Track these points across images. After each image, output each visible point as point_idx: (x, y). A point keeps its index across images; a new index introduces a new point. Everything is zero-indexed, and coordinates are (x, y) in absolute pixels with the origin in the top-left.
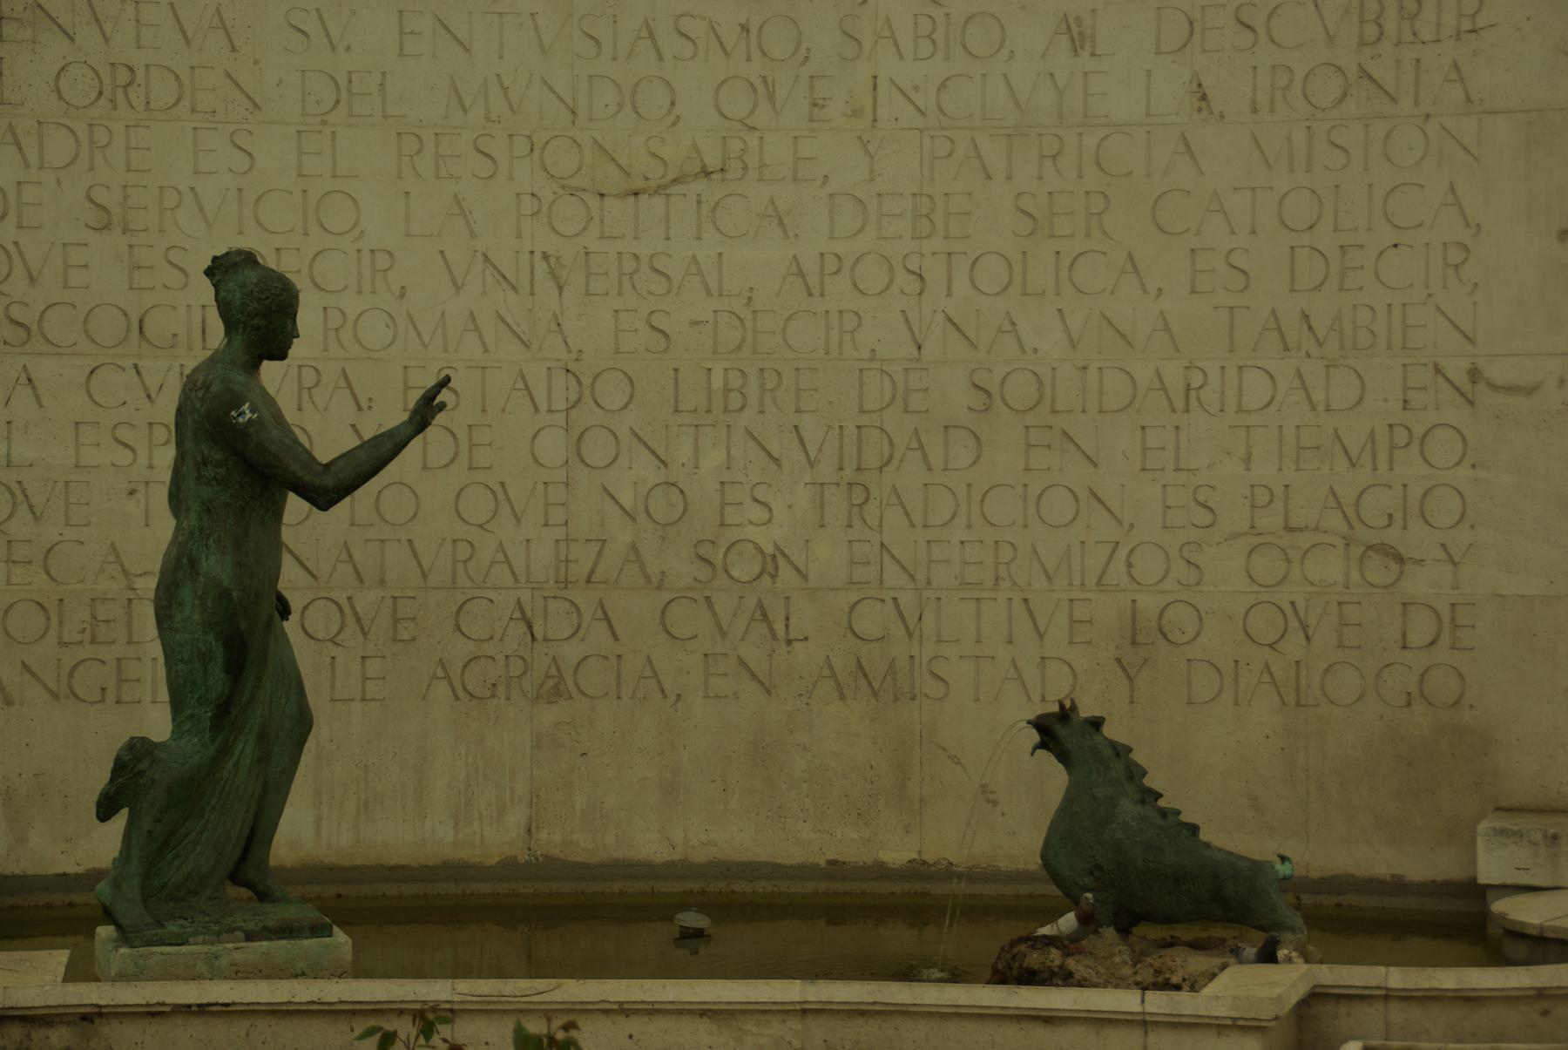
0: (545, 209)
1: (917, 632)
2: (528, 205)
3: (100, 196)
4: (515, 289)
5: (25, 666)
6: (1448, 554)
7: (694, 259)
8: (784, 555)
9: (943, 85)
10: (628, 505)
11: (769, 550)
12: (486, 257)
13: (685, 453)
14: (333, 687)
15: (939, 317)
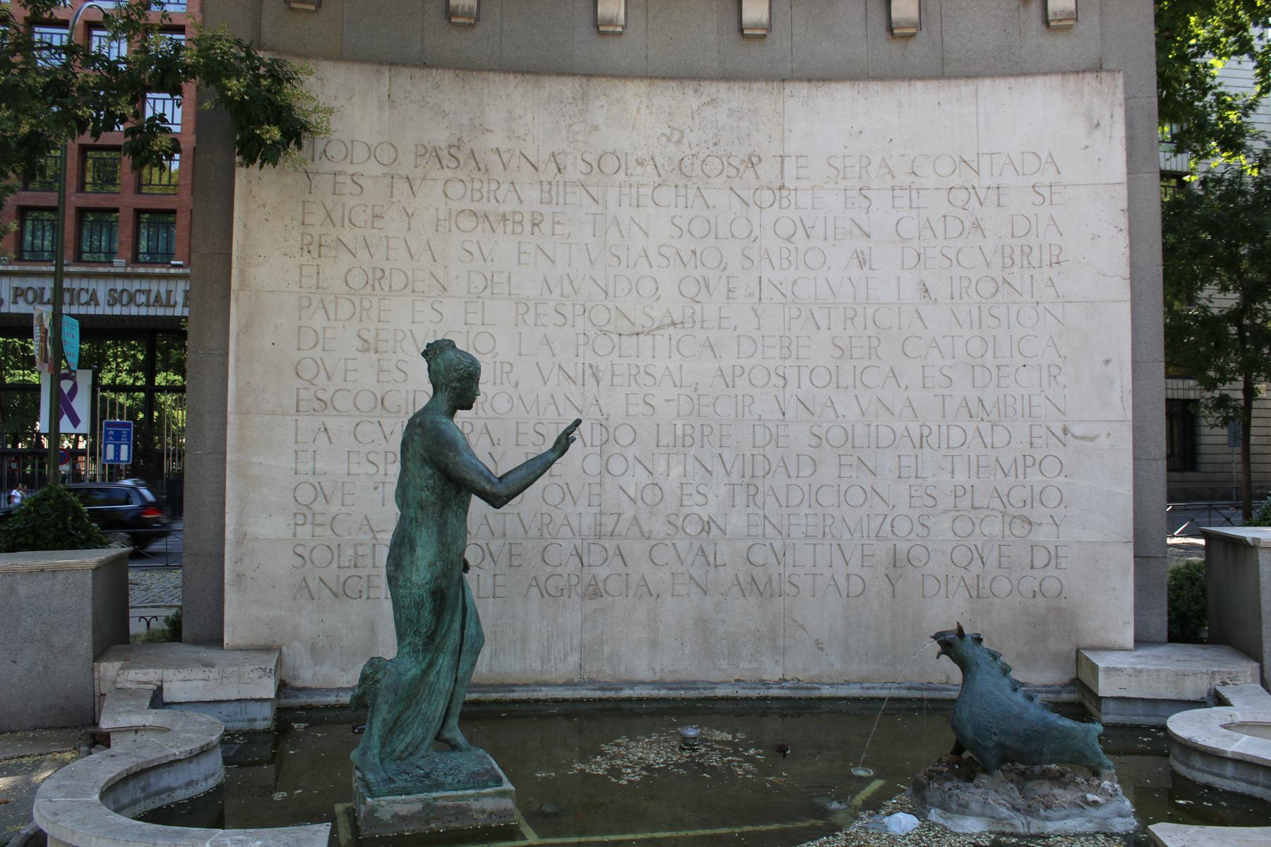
0: (591, 341)
1: (782, 562)
2: (582, 339)
3: (365, 335)
4: (575, 383)
5: (321, 580)
6: (1054, 521)
7: (668, 368)
8: (714, 521)
9: (795, 282)
10: (632, 495)
11: (706, 519)
12: (560, 367)
14: (478, 590)
15: (794, 399)
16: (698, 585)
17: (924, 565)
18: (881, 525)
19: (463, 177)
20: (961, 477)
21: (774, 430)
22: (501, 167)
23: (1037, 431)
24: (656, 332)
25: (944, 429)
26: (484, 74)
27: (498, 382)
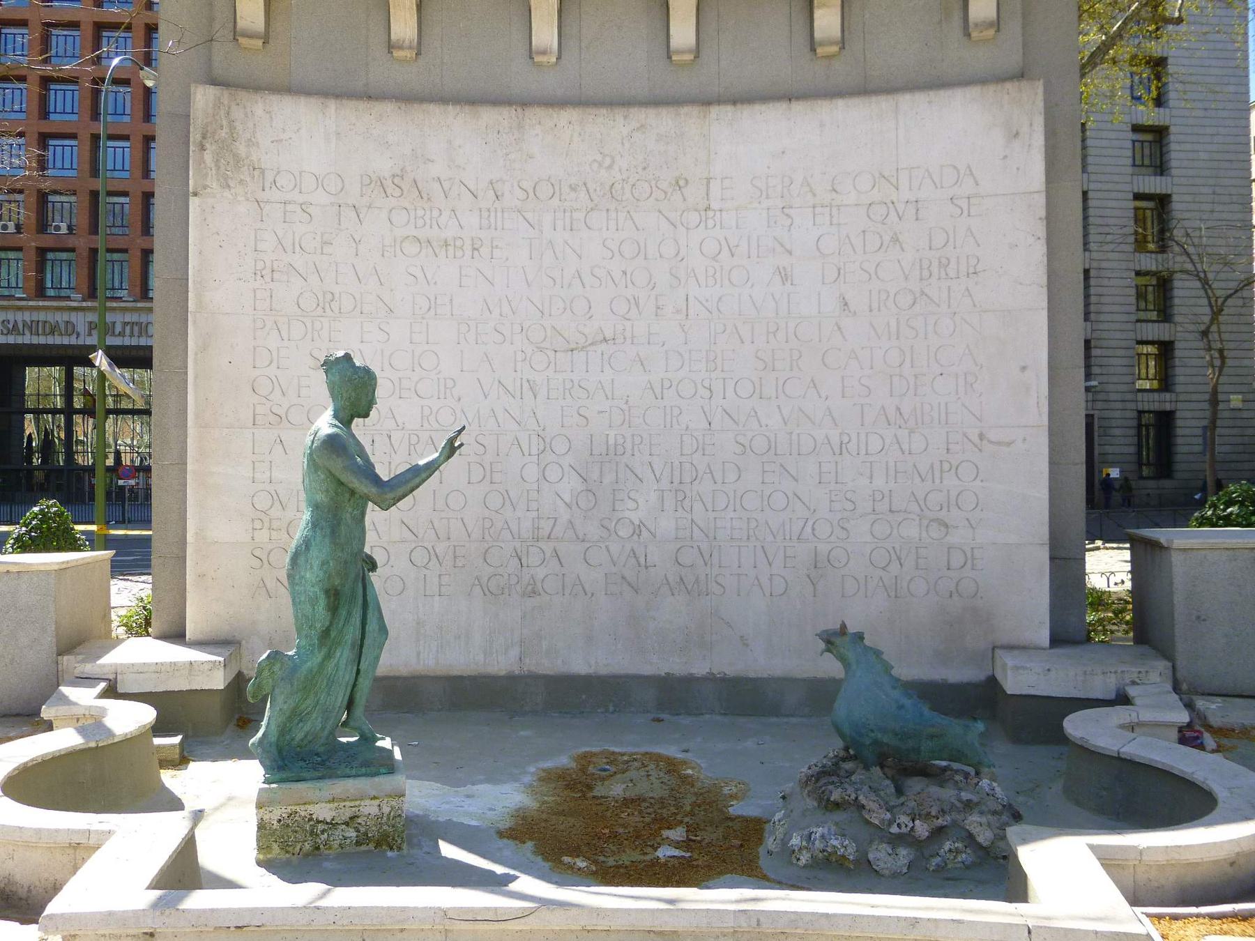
0: (528, 359)
7: (600, 382)
9: (720, 298)
10: (568, 500)
11: (637, 522)
12: (500, 382)
14: (425, 590)
15: (720, 409)
16: (629, 584)
17: (845, 566)
18: (803, 528)
19: (407, 205)
20: (879, 482)
21: (700, 438)
22: (443, 195)
24: (588, 348)
25: (863, 437)
26: (425, 106)
27: (442, 396)
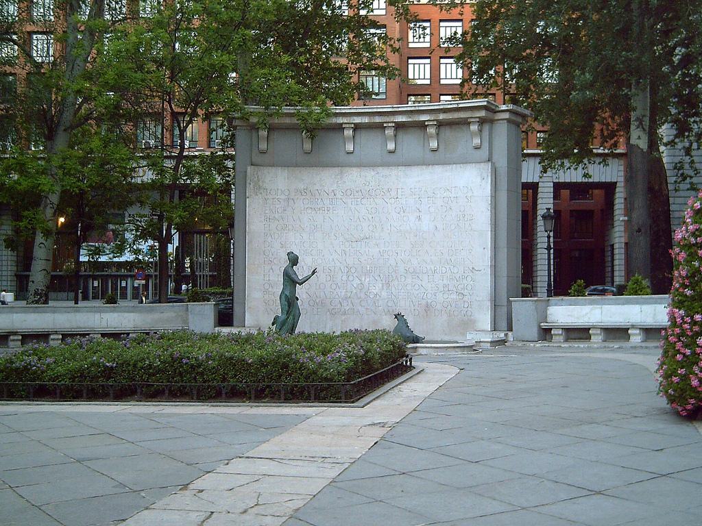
13: (363, 279)
20: (445, 282)
23: (465, 269)
